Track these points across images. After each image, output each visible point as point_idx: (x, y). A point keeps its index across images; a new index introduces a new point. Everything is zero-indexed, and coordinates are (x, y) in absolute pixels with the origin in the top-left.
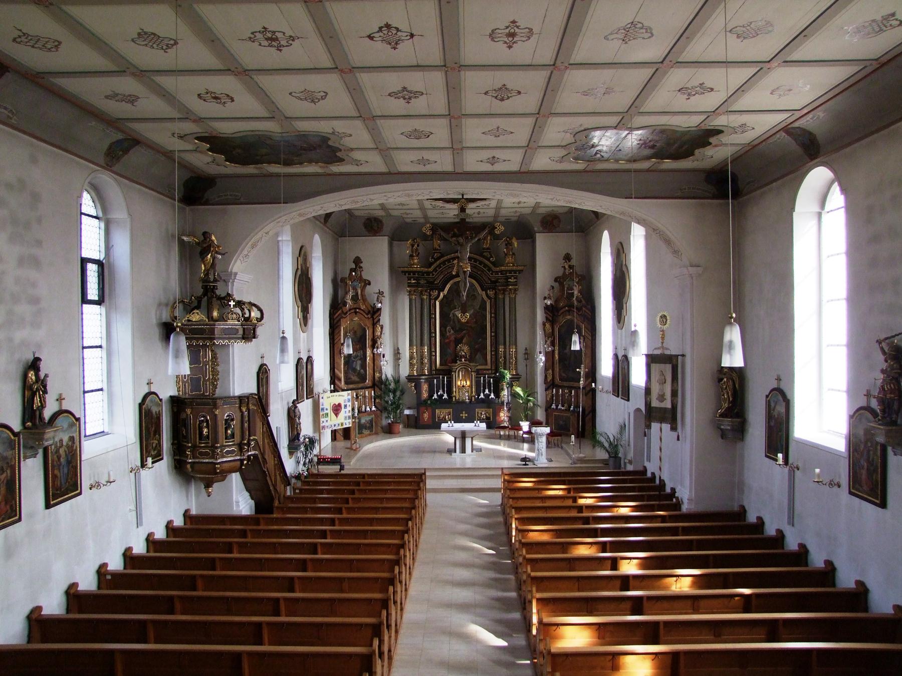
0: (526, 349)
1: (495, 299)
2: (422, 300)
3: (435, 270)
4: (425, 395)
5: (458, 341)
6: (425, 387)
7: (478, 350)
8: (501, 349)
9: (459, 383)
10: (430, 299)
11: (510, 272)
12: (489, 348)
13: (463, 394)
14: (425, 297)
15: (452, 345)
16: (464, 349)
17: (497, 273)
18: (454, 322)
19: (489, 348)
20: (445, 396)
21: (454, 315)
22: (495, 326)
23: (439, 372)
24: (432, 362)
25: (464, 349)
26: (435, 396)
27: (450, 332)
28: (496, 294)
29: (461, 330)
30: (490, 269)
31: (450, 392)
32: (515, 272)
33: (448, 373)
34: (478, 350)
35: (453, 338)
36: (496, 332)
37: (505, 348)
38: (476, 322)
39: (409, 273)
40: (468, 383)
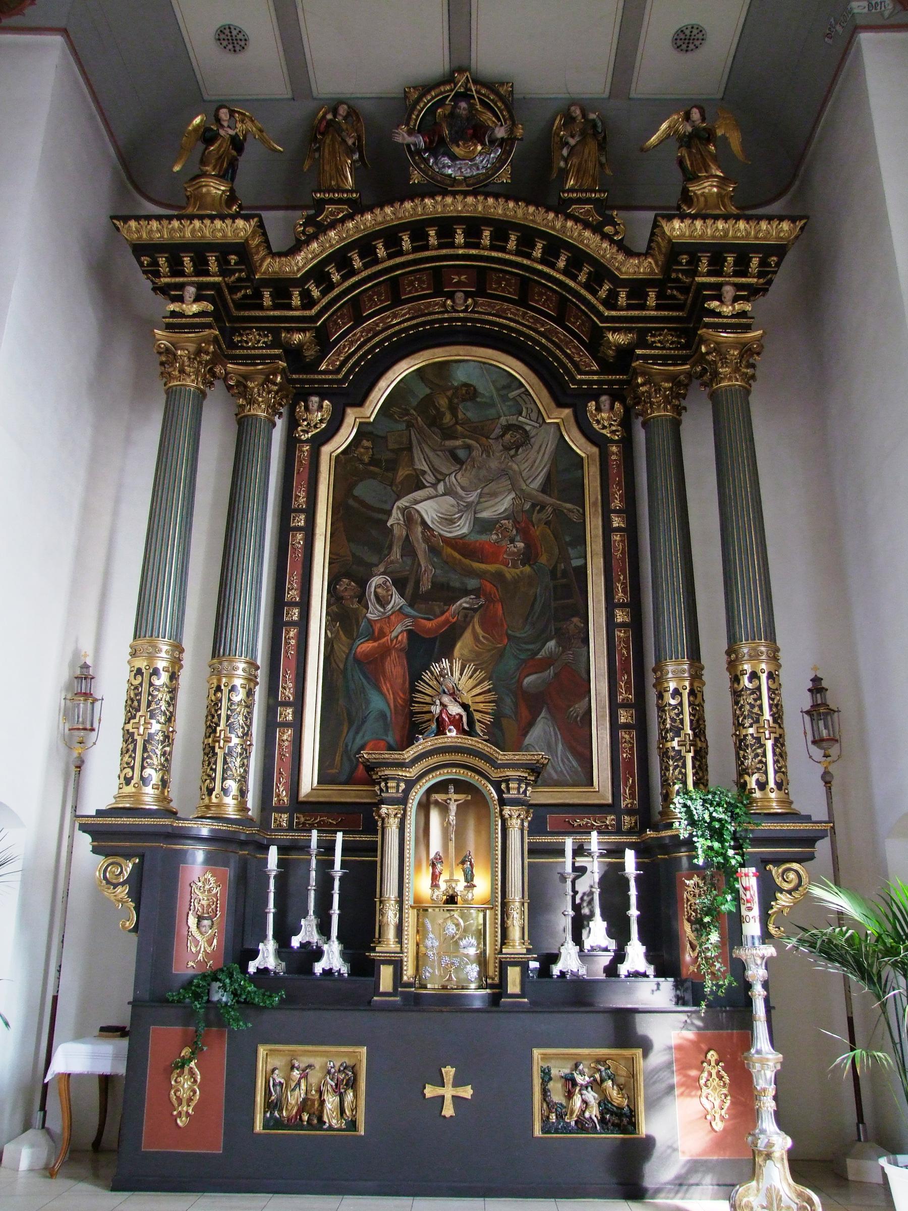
0: (817, 687)
1: (627, 443)
2: (244, 426)
3: (318, 273)
4: (199, 942)
5: (425, 650)
6: (201, 882)
7: (537, 696)
8: (676, 678)
9: (421, 884)
10: (291, 443)
11: (717, 252)
12: (599, 686)
13: (454, 943)
14: (261, 412)
15: (395, 668)
16: (459, 682)
17: (637, 288)
18: (408, 549)
19: (599, 686)
20: (332, 958)
21: (410, 517)
22: (627, 570)
23: (307, 811)
24: (278, 760)
25: (459, 682)
26: (267, 956)
27: (387, 607)
28: (626, 424)
29: (444, 593)
30: (601, 273)
31: (360, 934)
32: (743, 253)
33: (362, 821)
34: (537, 696)
35: (398, 632)
36: (635, 606)
37: (696, 675)
38: (528, 557)
39: (174, 251)
40: (483, 885)
